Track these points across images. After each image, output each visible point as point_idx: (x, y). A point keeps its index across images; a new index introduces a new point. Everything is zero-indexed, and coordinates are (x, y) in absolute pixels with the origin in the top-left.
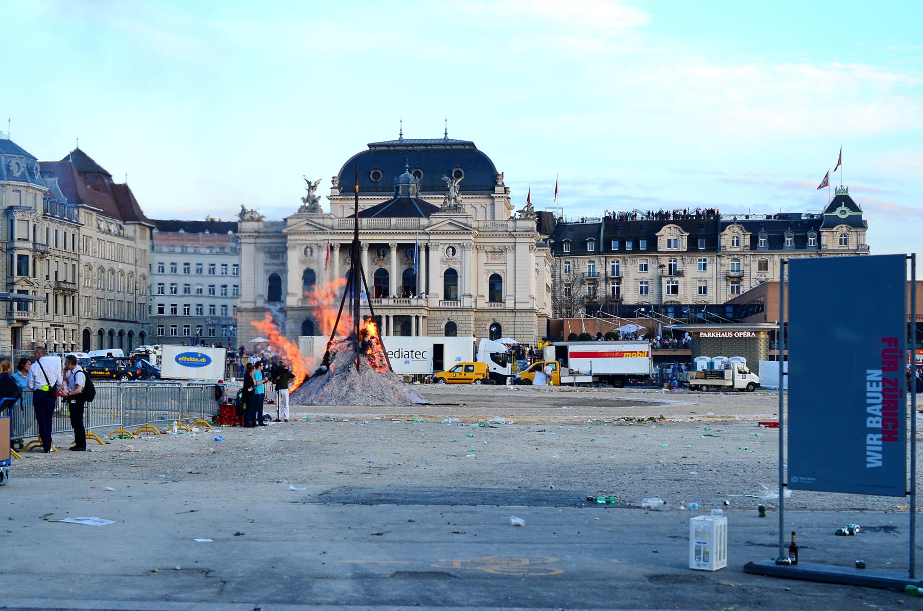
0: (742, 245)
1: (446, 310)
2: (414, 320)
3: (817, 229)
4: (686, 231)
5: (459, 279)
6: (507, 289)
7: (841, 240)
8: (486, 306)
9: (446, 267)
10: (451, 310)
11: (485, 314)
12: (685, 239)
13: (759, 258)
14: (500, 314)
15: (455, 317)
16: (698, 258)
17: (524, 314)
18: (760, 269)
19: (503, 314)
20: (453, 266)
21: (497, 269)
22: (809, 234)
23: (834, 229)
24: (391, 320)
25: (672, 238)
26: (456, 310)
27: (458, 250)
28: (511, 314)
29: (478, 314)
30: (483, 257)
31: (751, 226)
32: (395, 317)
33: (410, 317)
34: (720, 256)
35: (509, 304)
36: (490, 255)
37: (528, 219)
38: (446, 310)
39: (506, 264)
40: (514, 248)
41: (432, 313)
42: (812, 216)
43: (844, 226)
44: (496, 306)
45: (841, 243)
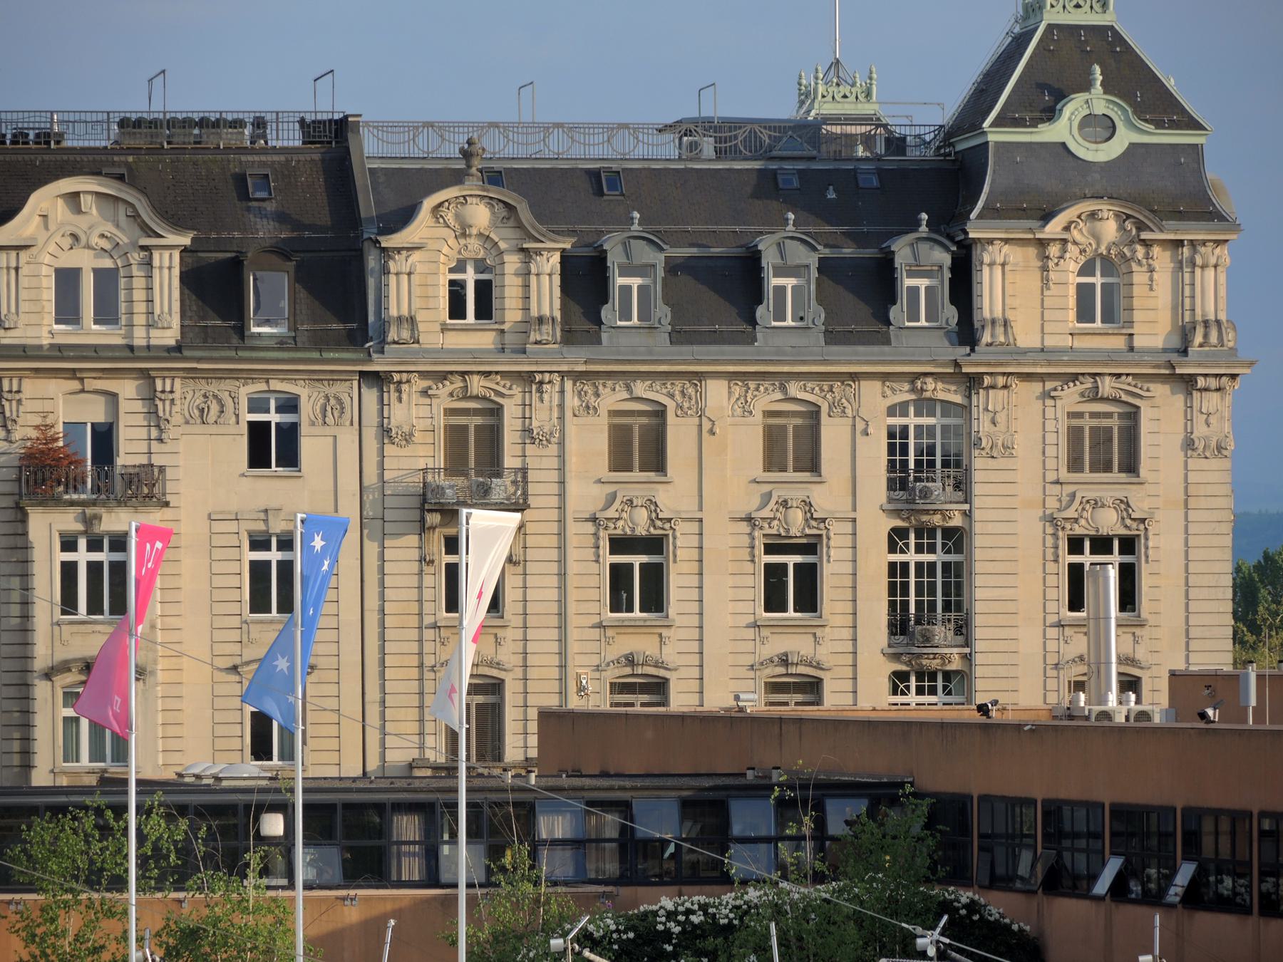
0: (510, 308)
3: (949, 223)
4: (178, 224)
7: (1085, 293)
12: (168, 268)
13: (612, 398)
16: (246, 391)
18: (620, 461)
22: (902, 250)
23: (1054, 228)
25: (86, 261)
31: (570, 200)
34: (377, 379)
42: (896, 144)
43: (1106, 209)
45: (1085, 313)
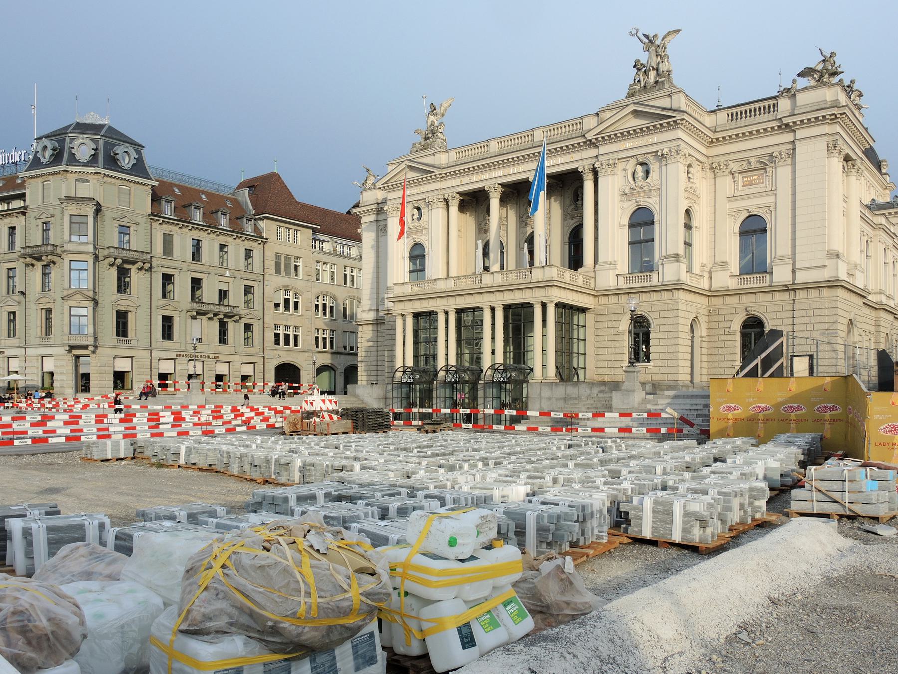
1: (627, 292)
2: (538, 311)
5: (656, 225)
6: (778, 243)
8: (733, 284)
9: (631, 207)
10: (638, 292)
11: (729, 300)
14: (761, 297)
15: (644, 305)
17: (813, 293)
19: (768, 296)
20: (644, 202)
21: (754, 205)
24: (500, 314)
26: (648, 291)
27: (654, 167)
28: (786, 296)
29: (714, 301)
30: (726, 185)
32: (507, 307)
33: (529, 306)
35: (781, 274)
36: (739, 177)
37: (825, 84)
38: (627, 292)
39: (773, 191)
40: (793, 154)
41: (603, 300)
44: (755, 282)
